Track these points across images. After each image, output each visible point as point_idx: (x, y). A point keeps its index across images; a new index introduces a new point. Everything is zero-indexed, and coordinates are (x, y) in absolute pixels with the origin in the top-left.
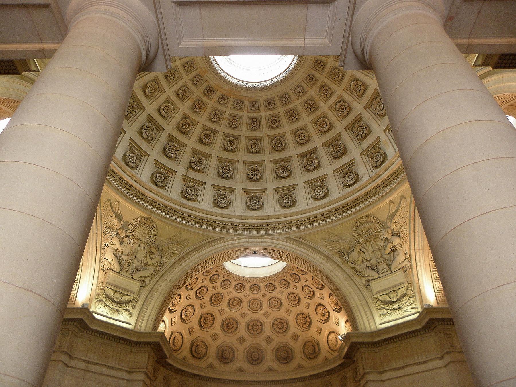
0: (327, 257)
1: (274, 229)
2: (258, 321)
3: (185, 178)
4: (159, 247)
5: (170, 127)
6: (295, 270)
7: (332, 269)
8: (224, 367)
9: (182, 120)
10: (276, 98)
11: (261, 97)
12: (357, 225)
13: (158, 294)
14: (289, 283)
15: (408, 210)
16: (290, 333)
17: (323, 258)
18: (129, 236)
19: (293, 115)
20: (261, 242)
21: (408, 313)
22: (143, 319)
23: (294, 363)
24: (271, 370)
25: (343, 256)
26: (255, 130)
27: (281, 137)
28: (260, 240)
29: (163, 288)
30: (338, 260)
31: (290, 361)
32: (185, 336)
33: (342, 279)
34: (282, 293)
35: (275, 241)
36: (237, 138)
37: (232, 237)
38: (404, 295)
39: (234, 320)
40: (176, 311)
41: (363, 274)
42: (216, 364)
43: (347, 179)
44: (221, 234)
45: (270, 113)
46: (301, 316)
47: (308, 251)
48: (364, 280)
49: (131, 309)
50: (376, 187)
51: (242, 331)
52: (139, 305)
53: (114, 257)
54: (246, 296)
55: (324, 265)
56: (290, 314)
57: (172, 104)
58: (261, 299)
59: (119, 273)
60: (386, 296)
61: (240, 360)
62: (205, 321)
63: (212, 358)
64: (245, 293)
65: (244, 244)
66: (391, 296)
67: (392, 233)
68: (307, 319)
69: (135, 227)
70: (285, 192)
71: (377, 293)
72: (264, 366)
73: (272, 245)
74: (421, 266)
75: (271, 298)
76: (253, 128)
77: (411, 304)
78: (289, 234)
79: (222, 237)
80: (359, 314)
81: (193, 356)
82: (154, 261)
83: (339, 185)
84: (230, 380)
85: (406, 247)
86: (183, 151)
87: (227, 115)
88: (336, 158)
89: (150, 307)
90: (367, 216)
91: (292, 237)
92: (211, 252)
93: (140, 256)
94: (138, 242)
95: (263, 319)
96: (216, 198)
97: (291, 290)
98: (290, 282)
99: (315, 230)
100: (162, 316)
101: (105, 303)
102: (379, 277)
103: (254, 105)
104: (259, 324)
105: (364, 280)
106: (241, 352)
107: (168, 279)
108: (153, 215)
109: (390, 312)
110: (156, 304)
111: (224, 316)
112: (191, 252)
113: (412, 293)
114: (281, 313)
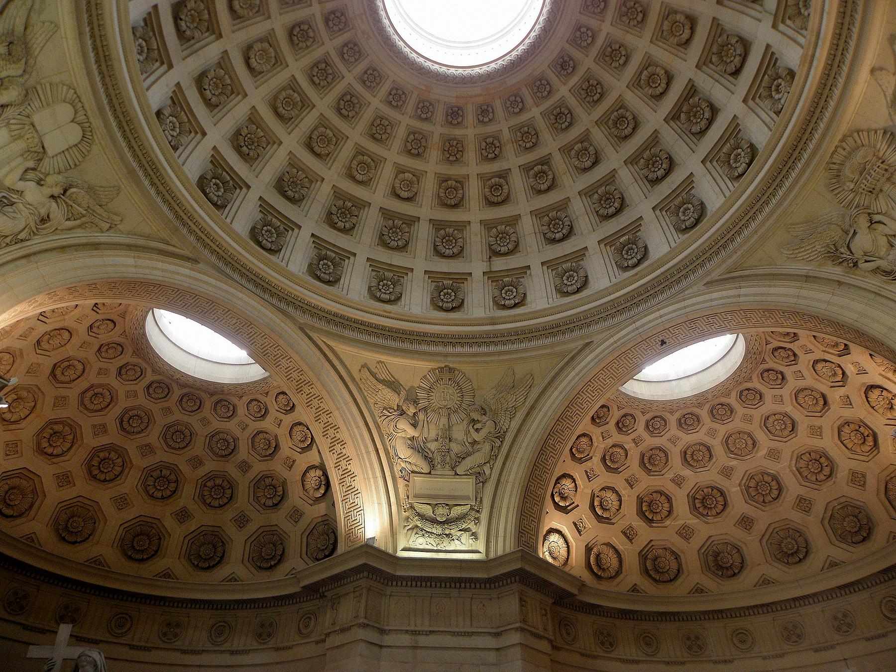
0: (808, 278)
1: (678, 281)
2: (764, 473)
3: (490, 275)
4: (485, 406)
5: (426, 209)
6: (769, 339)
7: (827, 297)
8: (729, 585)
10: (567, 46)
11: (542, 64)
13: (509, 485)
14: (782, 373)
16: (842, 474)
17: (798, 284)
18: (425, 409)
20: (661, 317)
22: (497, 537)
24: (833, 565)
25: (839, 257)
26: (567, 128)
27: (620, 108)
28: (657, 314)
29: (516, 473)
30: (835, 271)
31: (869, 534)
32: (620, 548)
36: (545, 161)
39: (713, 488)
40: (578, 506)
42: (709, 582)
44: (582, 338)
45: (574, 80)
46: (846, 430)
47: (759, 286)
49: (472, 526)
51: (739, 505)
52: (484, 516)
53: (412, 450)
54: (712, 433)
55: (805, 298)
57: (409, 172)
58: (746, 427)
59: (430, 473)
61: (759, 563)
62: (651, 508)
63: (695, 573)
64: (704, 429)
65: (630, 336)
68: (862, 430)
69: (430, 390)
70: (677, 201)
72: (815, 561)
73: (683, 311)
76: (564, 126)
78: (708, 273)
79: (588, 344)
81: (655, 580)
82: (483, 433)
83: (768, 120)
84: (748, 608)
88: (736, 73)
89: (504, 511)
90: (843, 140)
92: (577, 378)
93: (458, 433)
94: (444, 412)
95: (772, 467)
97: (793, 384)
98: (782, 368)
99: (756, 237)
100: (538, 519)
101: (422, 530)
104: (767, 478)
106: (753, 546)
107: (520, 455)
108: (449, 359)
110: (512, 506)
111: (688, 487)
112: (543, 392)
114: (803, 440)
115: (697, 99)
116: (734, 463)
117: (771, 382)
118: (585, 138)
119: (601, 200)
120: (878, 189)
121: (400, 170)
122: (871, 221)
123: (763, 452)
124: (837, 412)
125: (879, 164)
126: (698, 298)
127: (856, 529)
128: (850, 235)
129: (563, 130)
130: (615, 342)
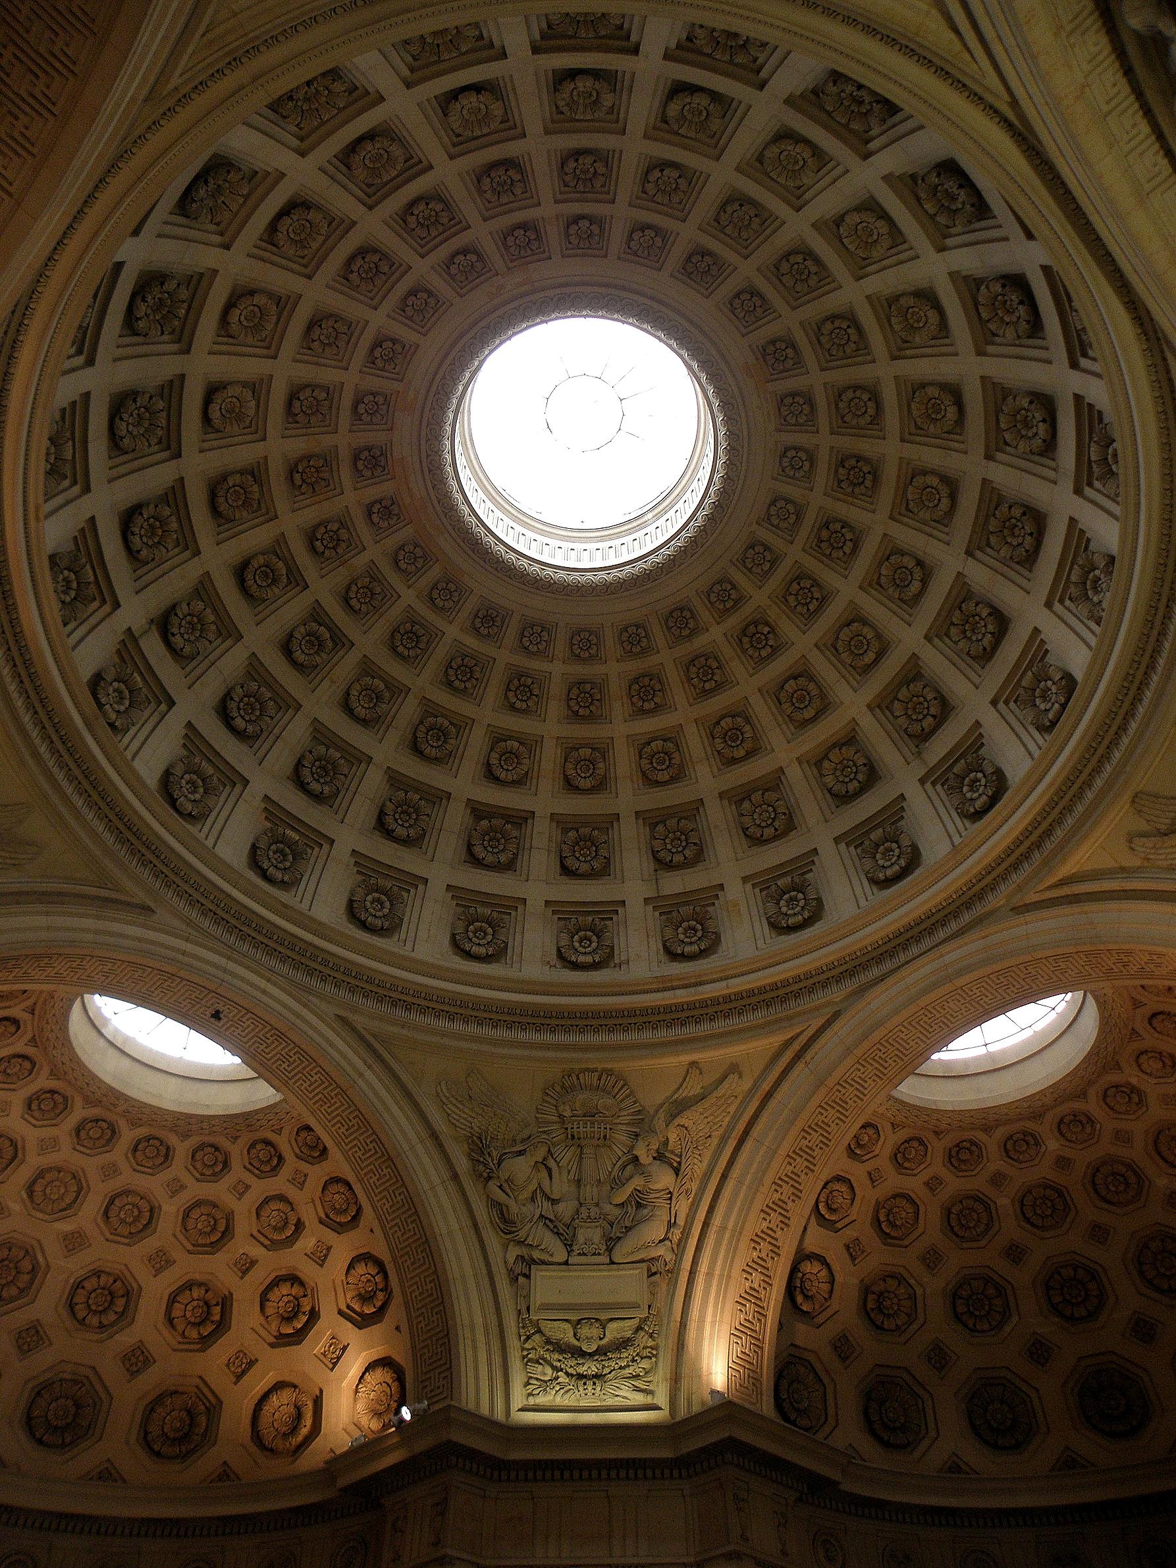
0: (434, 1136)
6: (285, 1131)
7: (436, 1180)
9: (242, 472)
12: (567, 1085)
15: (732, 1109)
16: (126, 1339)
19: (522, 691)
20: (264, 992)
21: (624, 1401)
23: (89, 1457)
26: (400, 655)
28: (263, 984)
33: (455, 1226)
34: (176, 1188)
35: (305, 1012)
36: (340, 641)
37: (176, 923)
38: (623, 1344)
41: (522, 1234)
43: (577, 945)
45: (471, 642)
48: (514, 1252)
50: (668, 1009)
54: (47, 1146)
55: (417, 1157)
56: (158, 1272)
60: (567, 1326)
66: (585, 1331)
67: (657, 1151)
71: (546, 1307)
73: (292, 1018)
74: (709, 1275)
75: (127, 1192)
77: (637, 1377)
79: (149, 909)
80: (470, 1354)
85: (682, 1207)
86: (176, 561)
87: (360, 561)
90: (609, 1072)
91: (359, 1027)
92: (90, 937)
96: (178, 771)
102: (566, 1263)
103: (445, 594)
104: (26, 1265)
105: (514, 1252)
109: (563, 1378)
113: (650, 1343)
114: (131, 1259)
115: (515, 833)
116: (16, 1207)
117: (199, 1165)
118: (397, 690)
119: (319, 760)
120: (583, 1142)
121: (258, 388)
122: (544, 1159)
123: (66, 1227)
124: (218, 1268)
125: (608, 1126)
126: (315, 1023)
127: (60, 1423)
128: (514, 1149)
129: (394, 649)
130: (184, 953)
